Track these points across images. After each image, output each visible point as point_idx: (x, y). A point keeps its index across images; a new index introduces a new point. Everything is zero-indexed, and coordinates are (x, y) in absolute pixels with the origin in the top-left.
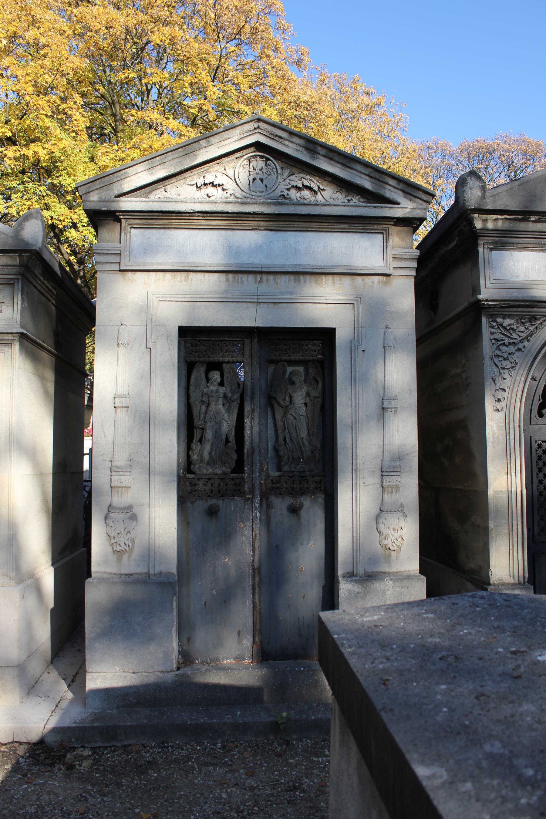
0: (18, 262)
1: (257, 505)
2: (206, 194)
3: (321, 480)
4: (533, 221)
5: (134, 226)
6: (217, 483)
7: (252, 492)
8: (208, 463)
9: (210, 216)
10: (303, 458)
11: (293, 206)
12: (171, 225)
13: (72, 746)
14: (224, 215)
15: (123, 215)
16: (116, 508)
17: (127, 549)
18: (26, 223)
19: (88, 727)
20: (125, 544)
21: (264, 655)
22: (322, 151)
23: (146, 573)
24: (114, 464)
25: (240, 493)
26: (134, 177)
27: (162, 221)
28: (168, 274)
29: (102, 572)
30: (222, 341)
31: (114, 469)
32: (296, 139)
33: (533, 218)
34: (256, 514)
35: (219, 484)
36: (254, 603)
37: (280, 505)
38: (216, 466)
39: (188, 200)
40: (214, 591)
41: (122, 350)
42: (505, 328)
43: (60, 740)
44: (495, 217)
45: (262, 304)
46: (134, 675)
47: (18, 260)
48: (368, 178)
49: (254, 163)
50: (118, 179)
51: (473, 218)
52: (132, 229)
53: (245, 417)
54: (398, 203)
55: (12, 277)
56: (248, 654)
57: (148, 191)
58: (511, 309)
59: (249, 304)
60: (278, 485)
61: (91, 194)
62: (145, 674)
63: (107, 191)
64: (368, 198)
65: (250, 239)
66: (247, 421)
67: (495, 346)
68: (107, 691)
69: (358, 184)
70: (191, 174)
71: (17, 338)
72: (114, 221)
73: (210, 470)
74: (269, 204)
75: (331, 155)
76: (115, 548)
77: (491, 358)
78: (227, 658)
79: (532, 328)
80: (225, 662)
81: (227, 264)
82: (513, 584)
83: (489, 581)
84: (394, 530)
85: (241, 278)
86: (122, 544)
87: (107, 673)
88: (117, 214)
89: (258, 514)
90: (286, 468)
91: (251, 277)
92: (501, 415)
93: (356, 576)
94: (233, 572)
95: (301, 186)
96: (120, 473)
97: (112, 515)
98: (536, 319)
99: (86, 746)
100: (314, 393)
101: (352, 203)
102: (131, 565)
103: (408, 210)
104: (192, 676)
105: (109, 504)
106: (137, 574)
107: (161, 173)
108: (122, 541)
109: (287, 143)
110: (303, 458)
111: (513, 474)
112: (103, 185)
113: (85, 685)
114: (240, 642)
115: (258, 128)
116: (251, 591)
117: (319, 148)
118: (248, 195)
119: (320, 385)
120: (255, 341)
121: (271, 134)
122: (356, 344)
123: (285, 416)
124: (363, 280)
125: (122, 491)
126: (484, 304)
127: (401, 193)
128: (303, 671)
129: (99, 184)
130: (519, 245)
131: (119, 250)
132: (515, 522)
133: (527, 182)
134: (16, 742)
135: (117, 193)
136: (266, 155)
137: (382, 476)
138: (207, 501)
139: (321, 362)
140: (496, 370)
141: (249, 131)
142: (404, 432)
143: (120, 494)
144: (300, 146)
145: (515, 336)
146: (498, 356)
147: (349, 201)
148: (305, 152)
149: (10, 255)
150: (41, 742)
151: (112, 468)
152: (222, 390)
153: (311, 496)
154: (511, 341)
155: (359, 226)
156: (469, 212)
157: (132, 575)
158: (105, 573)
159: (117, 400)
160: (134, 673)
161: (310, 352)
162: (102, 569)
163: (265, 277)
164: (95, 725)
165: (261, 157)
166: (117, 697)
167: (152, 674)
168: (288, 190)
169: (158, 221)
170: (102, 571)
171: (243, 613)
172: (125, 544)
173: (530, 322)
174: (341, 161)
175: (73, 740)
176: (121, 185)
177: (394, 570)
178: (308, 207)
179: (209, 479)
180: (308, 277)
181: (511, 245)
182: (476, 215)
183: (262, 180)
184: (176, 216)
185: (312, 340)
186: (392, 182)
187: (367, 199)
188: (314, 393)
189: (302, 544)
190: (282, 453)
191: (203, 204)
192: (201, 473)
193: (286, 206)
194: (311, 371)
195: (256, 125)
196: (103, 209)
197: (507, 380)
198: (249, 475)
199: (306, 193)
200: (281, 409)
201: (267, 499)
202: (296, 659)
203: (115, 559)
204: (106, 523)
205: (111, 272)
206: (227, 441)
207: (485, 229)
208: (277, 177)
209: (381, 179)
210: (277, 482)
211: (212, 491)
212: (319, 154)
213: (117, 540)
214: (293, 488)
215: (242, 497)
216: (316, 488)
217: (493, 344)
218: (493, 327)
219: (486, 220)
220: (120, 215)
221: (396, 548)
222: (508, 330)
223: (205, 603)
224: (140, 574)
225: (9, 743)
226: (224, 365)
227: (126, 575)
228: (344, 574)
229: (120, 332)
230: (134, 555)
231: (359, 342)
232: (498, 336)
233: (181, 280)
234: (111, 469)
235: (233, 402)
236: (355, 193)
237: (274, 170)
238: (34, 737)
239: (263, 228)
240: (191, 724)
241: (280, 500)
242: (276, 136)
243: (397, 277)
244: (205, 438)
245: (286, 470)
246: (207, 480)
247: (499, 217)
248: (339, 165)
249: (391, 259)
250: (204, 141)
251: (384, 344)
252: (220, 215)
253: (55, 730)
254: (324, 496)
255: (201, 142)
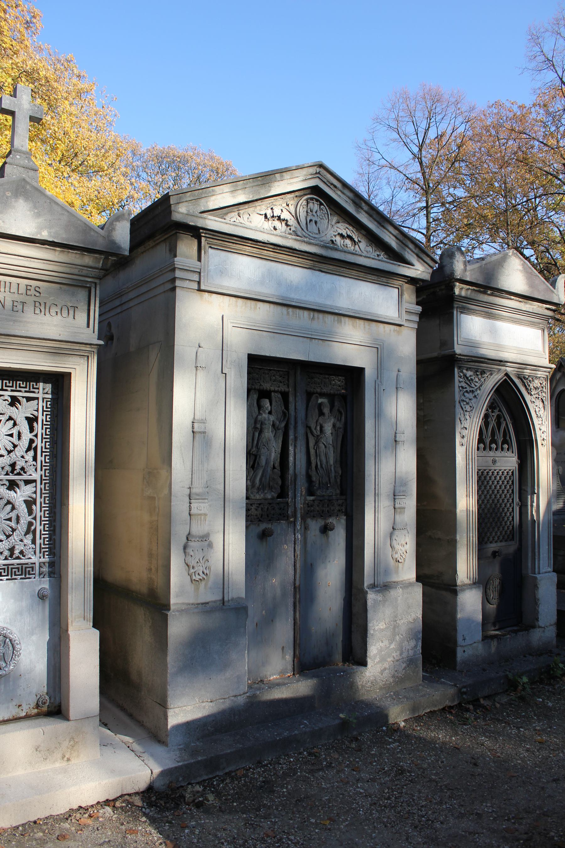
0: (101, 265)
1: (299, 528)
2: (273, 226)
3: (343, 503)
4: (489, 295)
5: (213, 246)
6: (266, 507)
7: (295, 516)
8: (259, 489)
9: (279, 250)
10: (330, 483)
11: (344, 253)
12: (245, 251)
13: (179, 785)
14: (291, 251)
15: (205, 233)
16: (195, 537)
17: (205, 577)
18: (118, 223)
19: (194, 762)
20: (203, 573)
21: (303, 666)
22: (366, 208)
23: (220, 600)
24: (194, 491)
25: (284, 516)
26: (219, 197)
27: (237, 246)
28: (240, 300)
29: (180, 604)
30: (270, 370)
31: (193, 496)
32: (347, 192)
33: (489, 292)
34: (298, 537)
35: (268, 509)
36: (295, 619)
37: (315, 526)
38: (266, 491)
39: (265, 231)
40: (264, 612)
41: (201, 374)
42: (467, 378)
43: (168, 782)
44: (468, 287)
45: (314, 340)
46: (211, 704)
47: (101, 262)
48: (394, 238)
49: (311, 205)
50: (206, 195)
51: (455, 286)
52: (210, 249)
53: (290, 445)
54: (413, 265)
55: (89, 280)
56: (290, 667)
57: (225, 212)
58: (471, 363)
59: (305, 339)
60: (312, 508)
61: (180, 205)
62: (221, 701)
63: (194, 205)
64: (391, 255)
65: (294, 275)
66: (291, 449)
67: (462, 393)
68: (188, 725)
69: (387, 242)
70: (261, 204)
71: (95, 351)
72: (192, 236)
73: (262, 495)
74: (205, 218)
75: (371, 212)
76: (194, 578)
77: (460, 402)
78: (273, 675)
79: (482, 380)
80: (272, 678)
81: (282, 296)
82: (470, 585)
83: (456, 583)
84: (401, 545)
85: (313, 316)
86: (201, 573)
87: (187, 707)
88: (201, 231)
89: (299, 536)
90: (319, 493)
91: (306, 313)
92: (464, 447)
93: (377, 587)
94: (279, 592)
95: (346, 235)
96: (199, 501)
97: (191, 544)
98: (485, 373)
99: (193, 782)
100: (338, 425)
101: (380, 258)
102: (209, 596)
103: (419, 272)
104: (260, 695)
105: (188, 532)
106: (212, 602)
107: (242, 198)
108: (200, 569)
109: (339, 193)
110: (330, 483)
111: (471, 497)
112: (193, 198)
113: (167, 722)
114: (283, 658)
115: (319, 173)
116: (292, 608)
117: (363, 204)
118: (307, 235)
119: (343, 418)
120: (299, 372)
121: (328, 181)
122: (380, 383)
123: (317, 443)
124: (384, 328)
125: (201, 518)
126: (457, 358)
127: (415, 256)
128: (343, 676)
129: (190, 196)
130: (477, 312)
131: (198, 268)
132: (471, 535)
133: (489, 263)
134: (125, 795)
135: (203, 209)
136: (321, 200)
137: (394, 499)
138: (259, 525)
139: (344, 398)
140: (462, 412)
141: (312, 174)
142: (406, 461)
143: (199, 522)
144: (349, 198)
145: (473, 385)
146: (463, 401)
147: (378, 255)
148: (352, 205)
149: (96, 255)
150: (150, 789)
151: (191, 495)
152: (272, 418)
153: (336, 518)
154: (471, 389)
155: (354, 273)
156: (453, 280)
157: (208, 603)
158: (183, 604)
159: (196, 425)
160: (211, 702)
161: (346, 387)
162: (180, 600)
163: (316, 314)
164: (199, 759)
165: (317, 200)
166: (197, 728)
167: (228, 700)
168: (335, 236)
169: (234, 245)
170: (180, 602)
171: (284, 631)
172: (203, 573)
173: (481, 375)
174: (378, 219)
175: (181, 779)
176: (207, 202)
177: (401, 579)
178: (355, 256)
179: (260, 504)
180: (347, 319)
181: (472, 311)
182: (457, 284)
183: (316, 222)
184: (251, 244)
185: (338, 376)
186: (411, 246)
187: (389, 256)
188: (338, 425)
189: (329, 562)
190: (314, 479)
191: (277, 237)
192: (255, 498)
193: (339, 252)
194: (336, 404)
195: (318, 170)
196: (190, 224)
197: (468, 421)
198: (292, 499)
199: (348, 242)
200: (313, 438)
201: (305, 522)
202: (324, 666)
203: (193, 589)
204: (185, 552)
205: (190, 290)
206: (274, 467)
207: (460, 296)
208: (328, 222)
209: (404, 242)
210: (312, 506)
211: (262, 515)
212: (362, 209)
213: (196, 569)
214: (323, 511)
215: (286, 520)
216: (339, 510)
217: (461, 390)
218: (460, 377)
219: (462, 289)
220: (203, 233)
221: (402, 561)
222: (469, 381)
223: (257, 624)
224: (215, 602)
225: (118, 798)
226: (273, 394)
227: (202, 604)
228: (368, 586)
229: (198, 354)
230: (210, 584)
231: (381, 382)
232: (464, 385)
233: (251, 307)
234: (190, 496)
235: (279, 430)
236: (381, 249)
237: (326, 216)
238: (142, 785)
239: (317, 269)
240: (280, 739)
241: (314, 522)
242: (332, 184)
243: (406, 328)
244: (258, 463)
245: (319, 494)
246: (258, 505)
247: (470, 287)
248: (376, 223)
249: (404, 312)
250: (279, 174)
251: (397, 385)
252: (288, 250)
253: (162, 774)
254: (345, 517)
255: (276, 175)
